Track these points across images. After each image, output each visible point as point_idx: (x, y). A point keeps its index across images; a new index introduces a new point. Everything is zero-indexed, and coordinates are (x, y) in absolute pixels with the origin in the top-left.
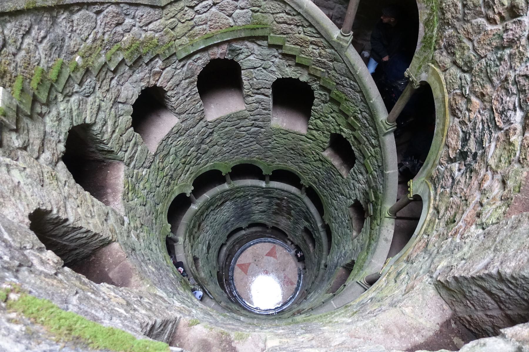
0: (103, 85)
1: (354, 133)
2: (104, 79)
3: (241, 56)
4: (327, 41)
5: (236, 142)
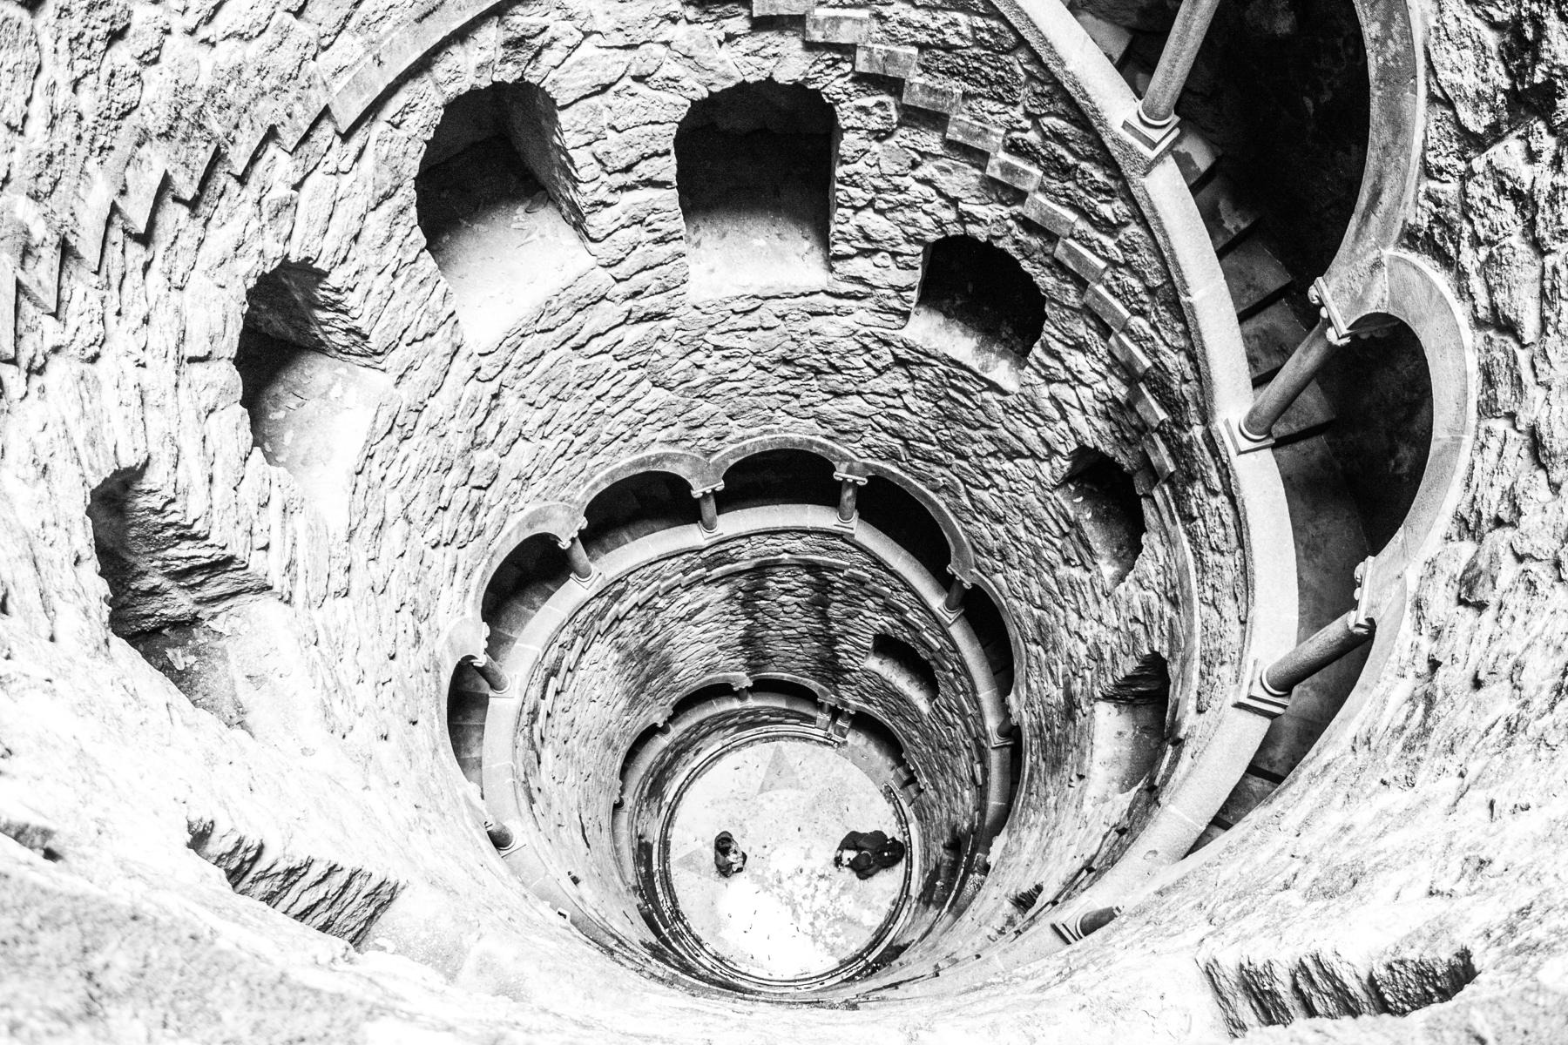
0: (125, 300)
1: (1018, 208)
2: (124, 276)
3: (549, 57)
5: (583, 403)
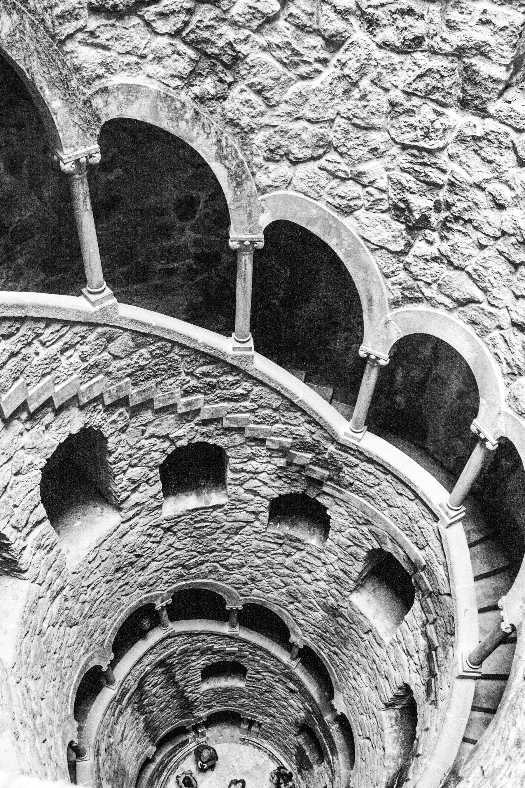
1: (198, 419)
4: (81, 324)
